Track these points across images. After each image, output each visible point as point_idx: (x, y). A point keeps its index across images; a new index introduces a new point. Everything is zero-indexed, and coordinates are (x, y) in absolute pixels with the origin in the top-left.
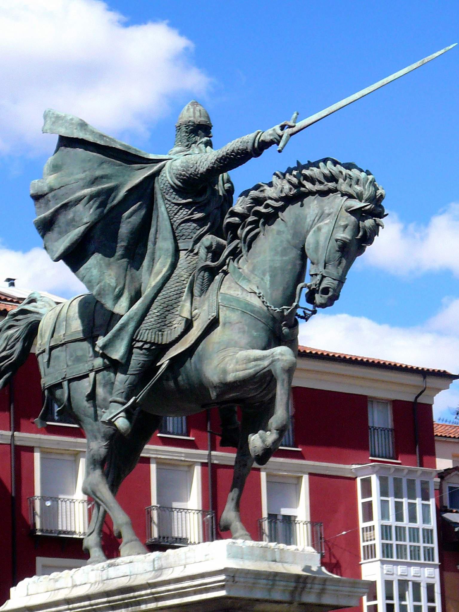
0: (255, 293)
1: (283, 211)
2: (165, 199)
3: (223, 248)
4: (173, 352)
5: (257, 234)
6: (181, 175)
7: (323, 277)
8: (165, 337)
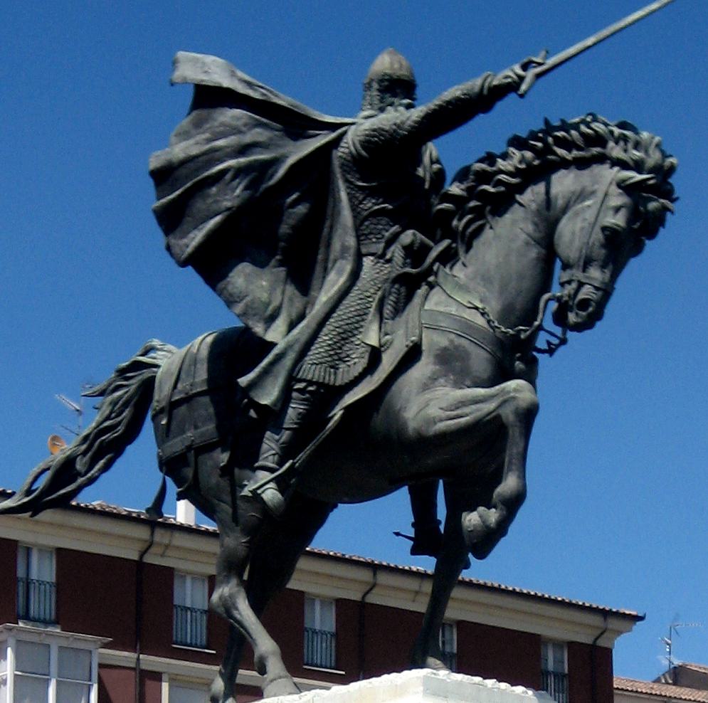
0: (477, 308)
1: (521, 192)
2: (346, 181)
3: (429, 249)
4: (350, 398)
7: (581, 285)
8: (340, 376)
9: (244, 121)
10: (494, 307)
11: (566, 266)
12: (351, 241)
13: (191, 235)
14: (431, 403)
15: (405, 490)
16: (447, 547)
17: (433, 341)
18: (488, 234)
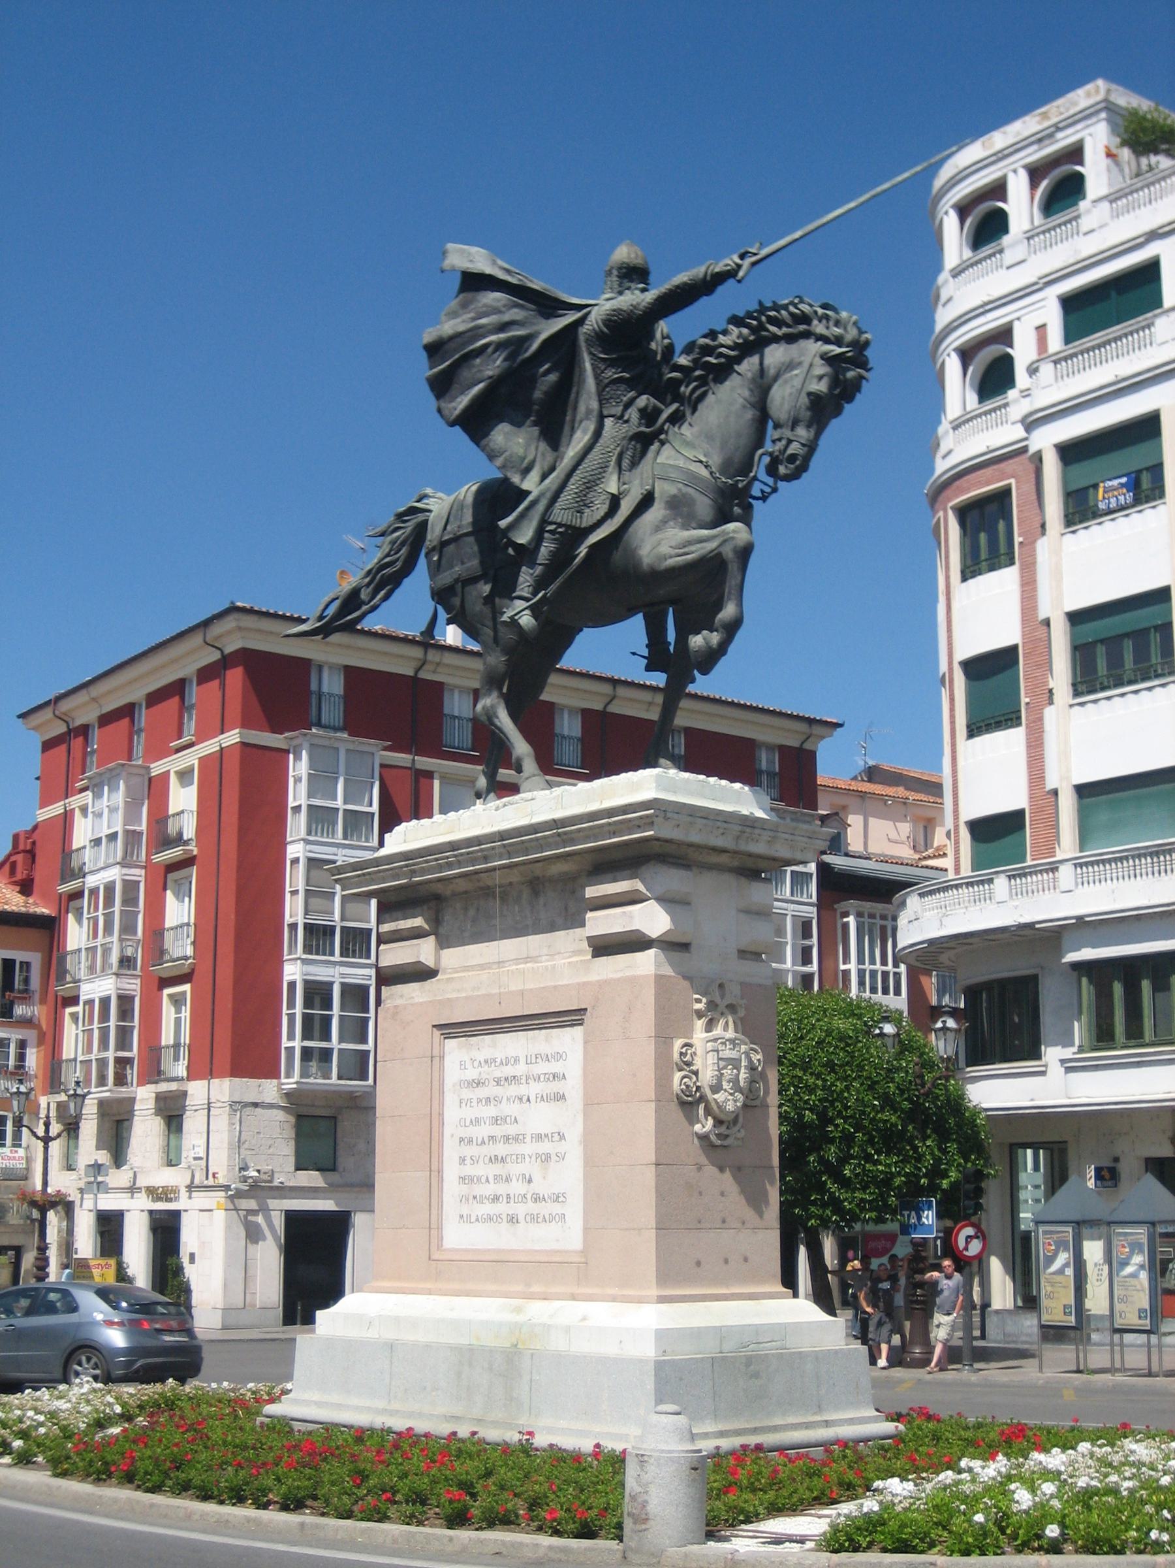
0: (701, 462)
1: (739, 363)
2: (591, 353)
3: (660, 412)
4: (594, 538)
6: (610, 320)
7: (790, 441)
8: (585, 519)
9: (503, 303)
10: (716, 460)
11: (777, 426)
12: (595, 405)
13: (459, 400)
14: (662, 543)
15: (640, 616)
16: (675, 664)
17: (663, 490)
18: (710, 398)
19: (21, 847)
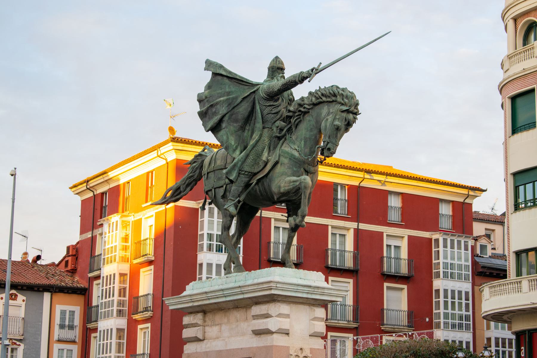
2: (259, 103)
5: (300, 121)
7: (328, 143)
14: (283, 181)
19: (70, 254)
